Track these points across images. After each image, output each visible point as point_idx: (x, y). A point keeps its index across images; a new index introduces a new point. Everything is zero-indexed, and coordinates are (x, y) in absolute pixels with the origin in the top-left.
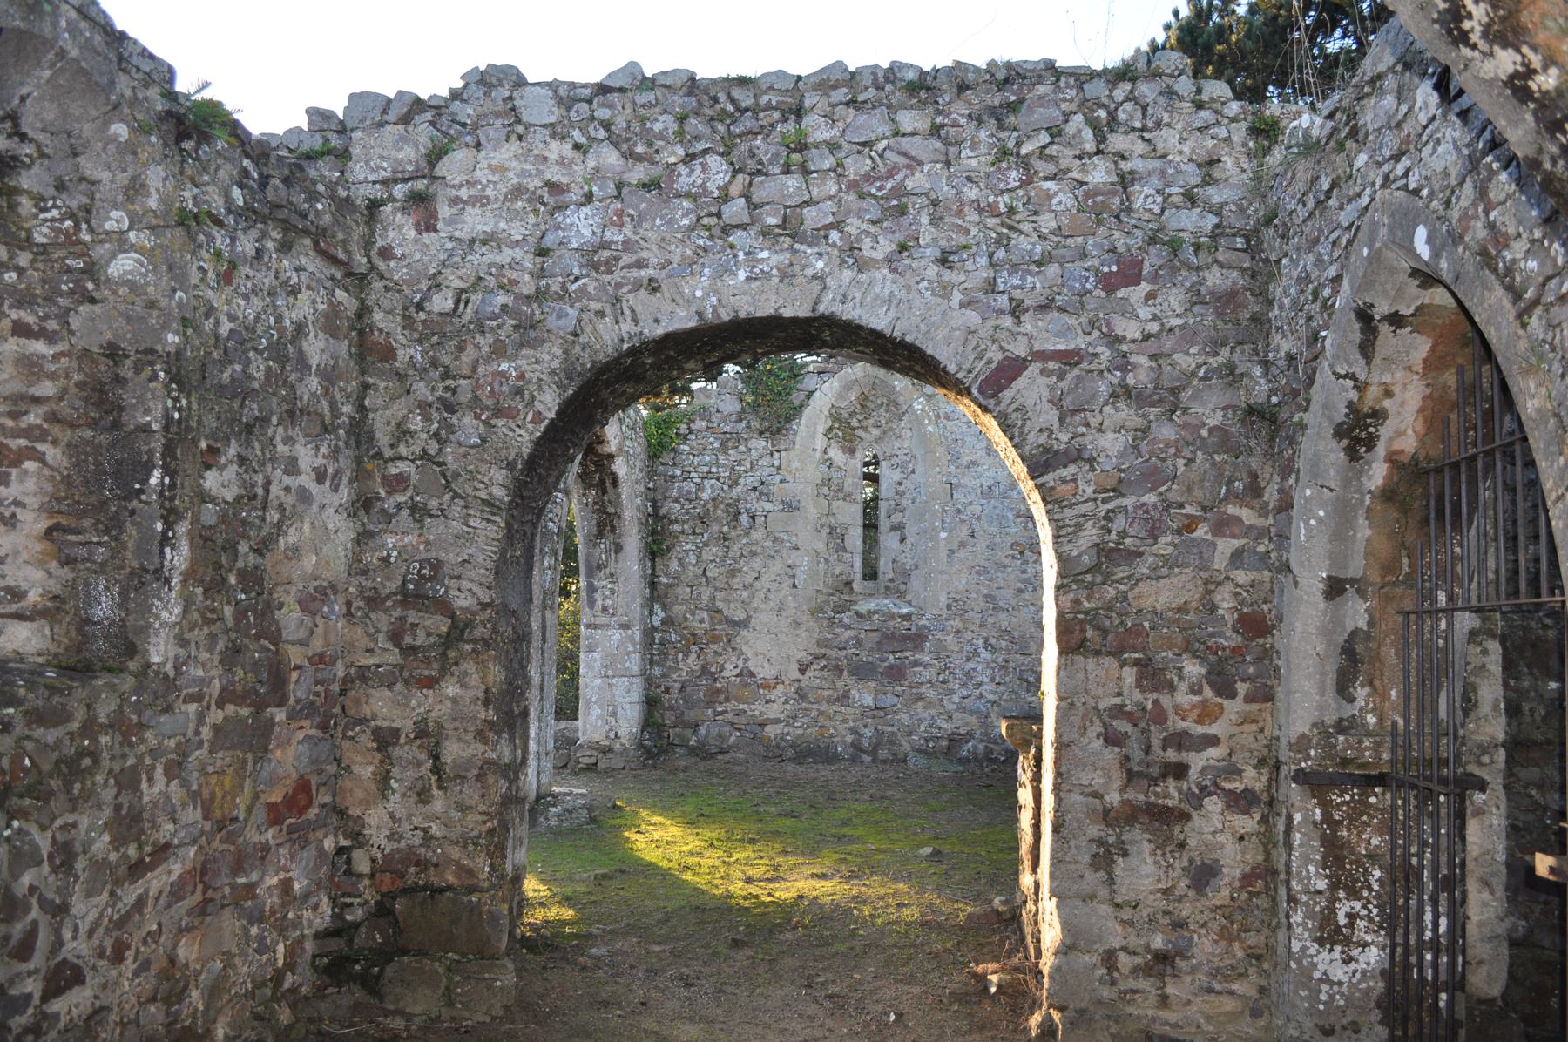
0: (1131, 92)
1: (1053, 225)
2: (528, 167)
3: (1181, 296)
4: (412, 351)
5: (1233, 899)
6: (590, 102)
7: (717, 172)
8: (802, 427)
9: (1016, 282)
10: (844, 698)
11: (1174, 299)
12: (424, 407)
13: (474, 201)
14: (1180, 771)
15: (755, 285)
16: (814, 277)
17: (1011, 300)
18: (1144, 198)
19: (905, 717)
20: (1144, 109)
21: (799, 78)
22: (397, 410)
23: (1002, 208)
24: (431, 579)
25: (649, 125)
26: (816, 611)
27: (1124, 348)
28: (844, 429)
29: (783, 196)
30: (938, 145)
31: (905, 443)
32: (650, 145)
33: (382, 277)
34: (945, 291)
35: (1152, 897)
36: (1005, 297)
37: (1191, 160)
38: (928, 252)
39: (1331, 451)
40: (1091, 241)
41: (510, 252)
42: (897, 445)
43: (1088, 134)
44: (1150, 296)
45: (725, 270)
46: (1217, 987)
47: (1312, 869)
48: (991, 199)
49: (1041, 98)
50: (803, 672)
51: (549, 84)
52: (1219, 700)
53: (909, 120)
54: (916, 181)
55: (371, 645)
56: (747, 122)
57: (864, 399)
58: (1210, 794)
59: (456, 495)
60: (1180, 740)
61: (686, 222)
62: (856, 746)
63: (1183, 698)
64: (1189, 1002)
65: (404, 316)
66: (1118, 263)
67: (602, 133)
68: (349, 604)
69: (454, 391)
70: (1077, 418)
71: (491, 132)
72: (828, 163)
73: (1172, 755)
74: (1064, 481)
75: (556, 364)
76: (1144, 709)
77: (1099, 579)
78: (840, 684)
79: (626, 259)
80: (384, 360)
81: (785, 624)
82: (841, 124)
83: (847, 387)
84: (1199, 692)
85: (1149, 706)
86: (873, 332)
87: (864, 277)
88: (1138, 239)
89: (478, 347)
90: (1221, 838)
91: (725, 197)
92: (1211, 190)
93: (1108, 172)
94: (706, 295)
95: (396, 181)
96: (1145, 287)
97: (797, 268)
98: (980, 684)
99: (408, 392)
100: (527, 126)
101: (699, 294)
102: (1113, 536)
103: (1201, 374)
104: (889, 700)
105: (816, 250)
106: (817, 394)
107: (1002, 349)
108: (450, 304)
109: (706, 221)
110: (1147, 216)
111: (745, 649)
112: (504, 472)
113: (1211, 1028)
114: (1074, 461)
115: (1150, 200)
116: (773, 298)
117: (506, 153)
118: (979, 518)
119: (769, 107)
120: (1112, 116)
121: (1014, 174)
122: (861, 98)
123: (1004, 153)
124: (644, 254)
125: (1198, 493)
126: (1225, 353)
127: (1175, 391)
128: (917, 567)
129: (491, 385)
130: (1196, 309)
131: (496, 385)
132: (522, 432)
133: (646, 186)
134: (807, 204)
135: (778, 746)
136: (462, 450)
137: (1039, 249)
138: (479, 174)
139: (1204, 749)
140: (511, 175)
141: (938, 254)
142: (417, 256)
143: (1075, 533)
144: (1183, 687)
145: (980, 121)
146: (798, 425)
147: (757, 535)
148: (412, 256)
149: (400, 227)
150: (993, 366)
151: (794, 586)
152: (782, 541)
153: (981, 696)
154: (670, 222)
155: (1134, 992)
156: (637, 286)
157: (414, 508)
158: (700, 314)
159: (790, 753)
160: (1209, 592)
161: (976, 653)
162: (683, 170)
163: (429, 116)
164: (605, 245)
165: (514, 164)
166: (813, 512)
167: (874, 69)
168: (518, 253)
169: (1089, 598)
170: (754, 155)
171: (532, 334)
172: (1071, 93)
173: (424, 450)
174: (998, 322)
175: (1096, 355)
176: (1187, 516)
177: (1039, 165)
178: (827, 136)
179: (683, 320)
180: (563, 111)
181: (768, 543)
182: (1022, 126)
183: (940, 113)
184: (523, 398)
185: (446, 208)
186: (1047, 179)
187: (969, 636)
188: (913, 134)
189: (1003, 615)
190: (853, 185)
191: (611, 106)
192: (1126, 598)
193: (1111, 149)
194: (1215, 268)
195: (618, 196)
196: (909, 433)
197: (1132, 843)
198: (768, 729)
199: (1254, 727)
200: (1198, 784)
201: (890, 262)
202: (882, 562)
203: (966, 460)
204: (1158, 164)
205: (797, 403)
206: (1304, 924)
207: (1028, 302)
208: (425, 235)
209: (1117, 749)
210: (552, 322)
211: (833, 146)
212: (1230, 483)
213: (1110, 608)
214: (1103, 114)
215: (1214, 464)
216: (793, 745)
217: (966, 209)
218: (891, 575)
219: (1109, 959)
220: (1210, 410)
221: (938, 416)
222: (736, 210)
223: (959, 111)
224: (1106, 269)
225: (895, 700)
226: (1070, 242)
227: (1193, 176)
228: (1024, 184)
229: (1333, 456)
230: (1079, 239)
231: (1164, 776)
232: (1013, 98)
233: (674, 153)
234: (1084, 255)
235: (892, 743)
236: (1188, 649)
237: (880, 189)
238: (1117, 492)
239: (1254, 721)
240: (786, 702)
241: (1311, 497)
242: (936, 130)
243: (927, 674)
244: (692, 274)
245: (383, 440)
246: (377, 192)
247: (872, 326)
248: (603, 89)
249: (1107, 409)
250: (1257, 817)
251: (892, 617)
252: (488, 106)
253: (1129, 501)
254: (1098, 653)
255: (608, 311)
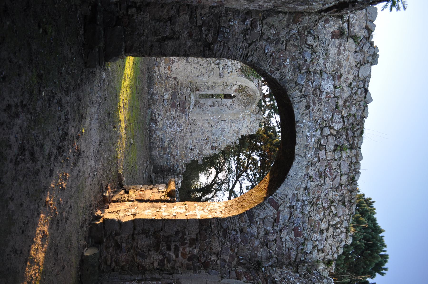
0: (343, 232)
1: (312, 215)
2: (347, 68)
3: (290, 246)
4: (295, 29)
5: (136, 262)
6: (363, 87)
7: (337, 126)
8: (243, 79)
9: (298, 207)
10: (166, 90)
11: (290, 245)
12: (278, 34)
13: (339, 51)
14: (169, 249)
15: (305, 138)
16: (306, 154)
17: (294, 206)
18: (316, 236)
19: (161, 108)
20: (339, 235)
21: (360, 148)
22: (277, 25)
23: (318, 202)
24: (224, 36)
25: (354, 106)
26: (191, 82)
27: (279, 233)
28: (242, 90)
29: (329, 145)
30: (337, 186)
31: (238, 107)
32: (348, 106)
33: (319, 19)
34: (298, 189)
35: (135, 243)
36: (295, 204)
37: (324, 246)
38: (309, 184)
40: (307, 224)
41: (322, 62)
42: (237, 105)
43: (334, 223)
44: (291, 239)
45: (310, 128)
46: (113, 259)
48: (321, 200)
49: (345, 211)
50: (174, 78)
51: (370, 75)
52: (187, 257)
53: (344, 179)
54: (328, 180)
55: (203, 15)
56: (350, 133)
57: (250, 96)
58: (163, 256)
59: (250, 45)
60: (176, 249)
61: (325, 117)
62: (153, 94)
63: (187, 250)
64: (108, 253)
65: (306, 27)
66: (301, 231)
67: (354, 92)
68: (216, 7)
69: (282, 44)
70: (261, 222)
71: (359, 57)
72: (336, 157)
73: (173, 247)
74: (245, 219)
75: (288, 77)
76: (185, 240)
77: (219, 228)
78: (170, 89)
79: (316, 99)
80: (294, 20)
81: (187, 73)
82: (346, 160)
83: (254, 92)
84: (189, 253)
85: (186, 241)
86: (289, 170)
87: (304, 167)
88: (306, 236)
89: (295, 52)
90: (152, 259)
91: (330, 128)
92: (316, 251)
93: (324, 227)
94: (303, 123)
95: (348, 24)
96: (294, 238)
97: (308, 149)
98: (171, 128)
99: (283, 28)
100: (359, 68)
101: (304, 121)
102: (230, 231)
103: (271, 251)
104: (166, 103)
105: (313, 154)
106: (252, 83)
107: (281, 204)
108: (309, 42)
109: (325, 123)
110: (311, 237)
111: (180, 61)
112: (256, 61)
113: (102, 258)
114: (250, 221)
115: (315, 237)
116: (301, 143)
117: (352, 61)
118: (216, 128)
119: (354, 140)
120: (338, 228)
121: (326, 205)
122: (352, 165)
123: (332, 202)
124: (317, 105)
125: (240, 251)
126: (275, 256)
127: (267, 245)
128: (203, 110)
129: (283, 56)
130: (287, 249)
131: (283, 58)
132: (268, 67)
133: (337, 106)
134: (326, 151)
135: (152, 71)
136: (263, 47)
137: (307, 212)
138: (347, 52)
139: (175, 254)
140: (346, 63)
141: (308, 187)
142: (325, 32)
143: (231, 222)
144: (191, 249)
145: (341, 196)
146: (244, 78)
147: (213, 65)
148: (325, 30)
149: (334, 26)
150: (277, 201)
151: (198, 76)
152: (211, 73)
153: (167, 128)
154: (325, 112)
155: (110, 240)
156: (308, 103)
157: (247, 30)
158: (298, 122)
159: (150, 75)
160: (215, 253)
161: (179, 127)
162: (340, 116)
163: (367, 36)
164: (321, 92)
165: (348, 64)
166: (219, 81)
167: (359, 168)
168: (322, 65)
169: (214, 226)
170: (341, 136)
171: (297, 70)
172: (345, 218)
173: (264, 34)
174: (288, 203)
175: (277, 226)
176: (235, 249)
177: (328, 211)
178: (343, 156)
179: (297, 116)
180: (362, 79)
181: (210, 68)
182: (338, 206)
183: (345, 186)
184: (278, 67)
185: (338, 42)
186: (324, 213)
187: (184, 125)
188: (341, 179)
189: (190, 134)
190: (329, 164)
191: (361, 94)
192: (214, 235)
193: (330, 228)
194: (296, 253)
195: (335, 96)
196: (240, 108)
197: (150, 239)
198: (157, 68)
199: (181, 265)
200: (166, 253)
201: (307, 174)
202: (204, 100)
203: (232, 124)
204: (324, 239)
205: (250, 77)
207: (293, 210)
208: (331, 34)
209: (174, 234)
210: (300, 76)
211: (340, 158)
212: (242, 259)
213: (212, 231)
214: (339, 226)
215: (248, 255)
216: (152, 76)
217: (319, 194)
218: (201, 102)
219: (117, 234)
220: (261, 254)
221: (244, 117)
222: (327, 131)
223: (344, 191)
224: (299, 228)
225: (166, 105)
226: (307, 219)
227: (320, 247)
228: (323, 208)
230: (307, 221)
231: (167, 245)
232: (346, 204)
233: (345, 113)
234: (303, 223)
235: (154, 104)
236: (200, 250)
237: (327, 171)
238: (242, 232)
239: (182, 266)
240: (165, 73)
242: (341, 185)
243: (173, 113)
244: (310, 119)
245: (269, 20)
246: (346, 18)
247: (290, 170)
248: (366, 91)
249: (263, 229)
250: (158, 267)
251: (189, 104)
252: (367, 55)
253: (239, 235)
254: (200, 229)
255: (302, 94)
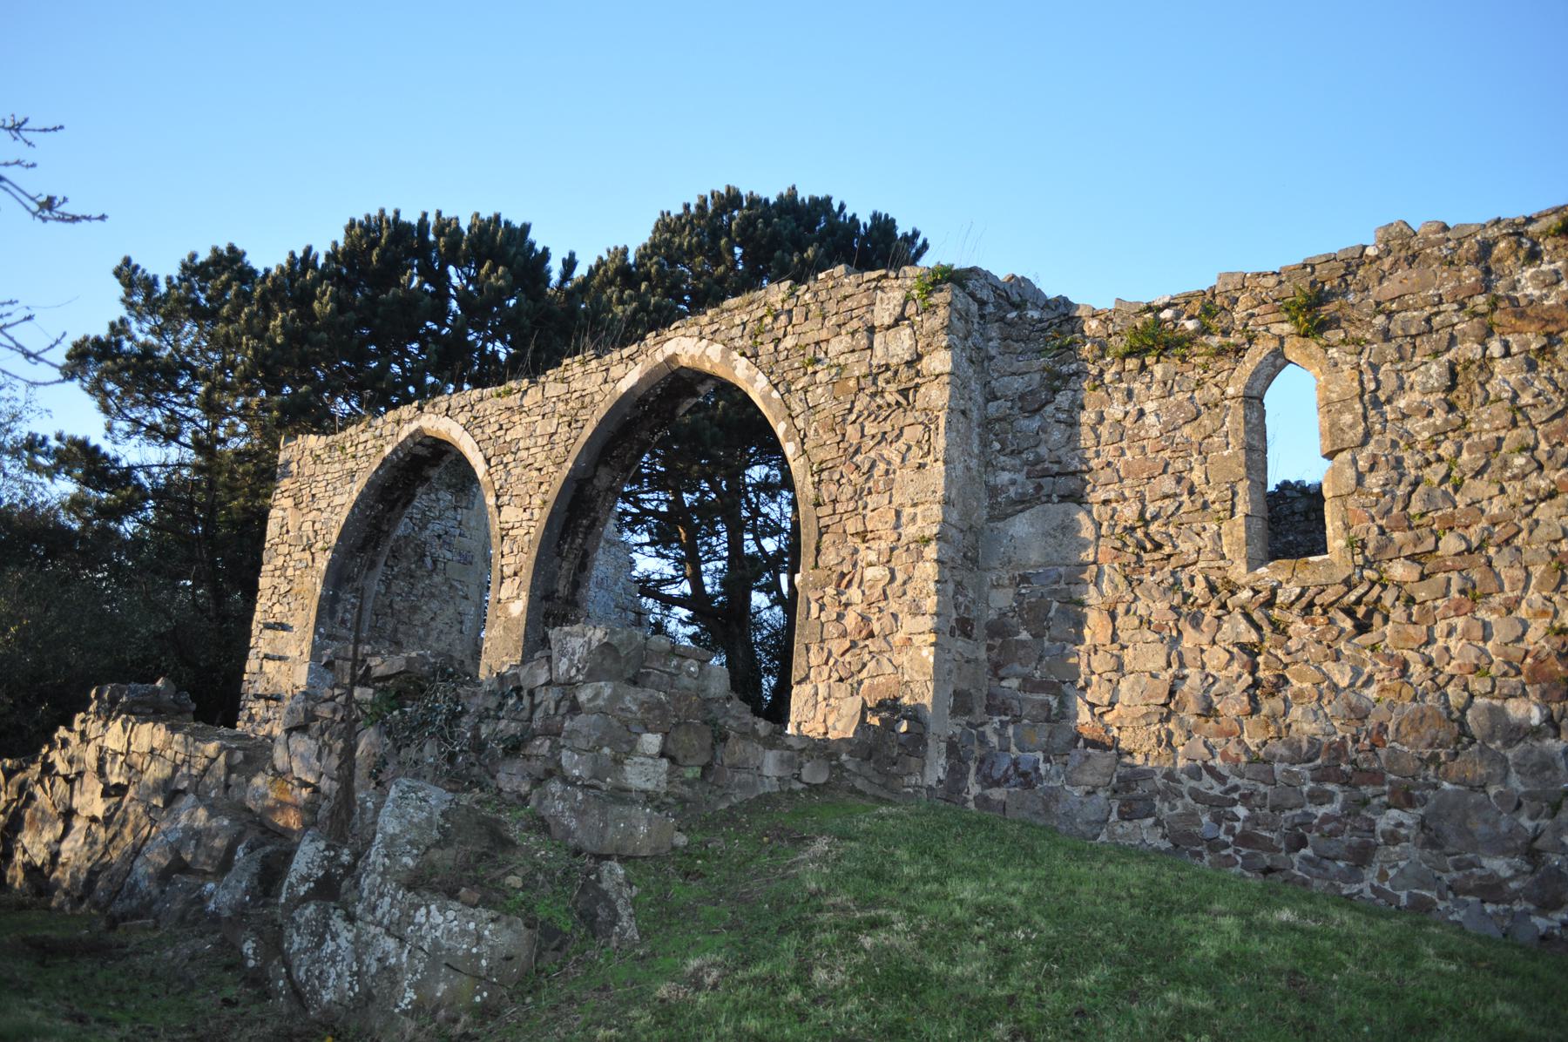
147: (437, 579)
151: (461, 632)
181: (445, 588)
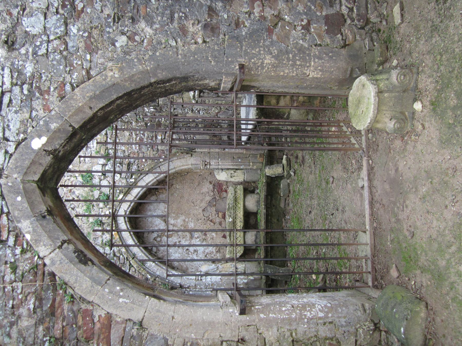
39: (91, 270)
47: (284, 309)
206: (310, 311)
229: (94, 271)
241: (109, 290)
